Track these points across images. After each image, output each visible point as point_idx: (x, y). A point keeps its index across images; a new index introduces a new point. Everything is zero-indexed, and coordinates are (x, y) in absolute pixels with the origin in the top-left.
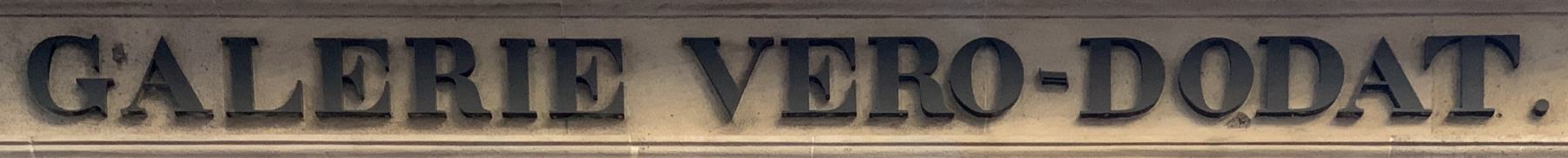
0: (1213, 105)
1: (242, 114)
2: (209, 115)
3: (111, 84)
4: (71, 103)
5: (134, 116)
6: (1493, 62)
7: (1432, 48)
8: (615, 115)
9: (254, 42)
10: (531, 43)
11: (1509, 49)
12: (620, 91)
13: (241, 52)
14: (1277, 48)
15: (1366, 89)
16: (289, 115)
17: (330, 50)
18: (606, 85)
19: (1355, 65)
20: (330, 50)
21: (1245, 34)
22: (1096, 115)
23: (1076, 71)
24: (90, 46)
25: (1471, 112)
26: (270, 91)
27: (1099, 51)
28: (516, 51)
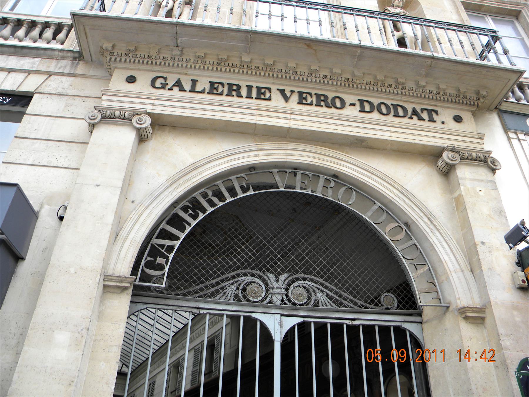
0: (385, 113)
1: (193, 90)
2: (186, 91)
3: (167, 84)
4: (159, 86)
5: (171, 89)
6: (434, 115)
7: (422, 110)
8: (269, 99)
9: (197, 81)
10: (253, 86)
11: (436, 112)
12: (270, 96)
13: (194, 82)
14: (395, 106)
15: (413, 114)
16: (203, 92)
17: (212, 84)
18: (268, 95)
19: (410, 111)
20: (212, 84)
21: (389, 103)
22: (362, 111)
23: (358, 104)
24: (165, 79)
25: (431, 120)
26: (199, 88)
27: (362, 102)
28: (250, 88)
